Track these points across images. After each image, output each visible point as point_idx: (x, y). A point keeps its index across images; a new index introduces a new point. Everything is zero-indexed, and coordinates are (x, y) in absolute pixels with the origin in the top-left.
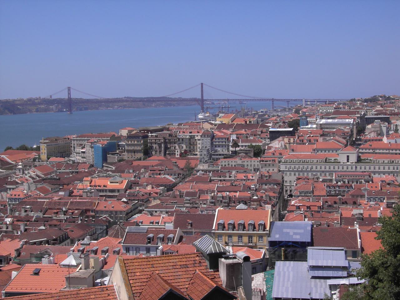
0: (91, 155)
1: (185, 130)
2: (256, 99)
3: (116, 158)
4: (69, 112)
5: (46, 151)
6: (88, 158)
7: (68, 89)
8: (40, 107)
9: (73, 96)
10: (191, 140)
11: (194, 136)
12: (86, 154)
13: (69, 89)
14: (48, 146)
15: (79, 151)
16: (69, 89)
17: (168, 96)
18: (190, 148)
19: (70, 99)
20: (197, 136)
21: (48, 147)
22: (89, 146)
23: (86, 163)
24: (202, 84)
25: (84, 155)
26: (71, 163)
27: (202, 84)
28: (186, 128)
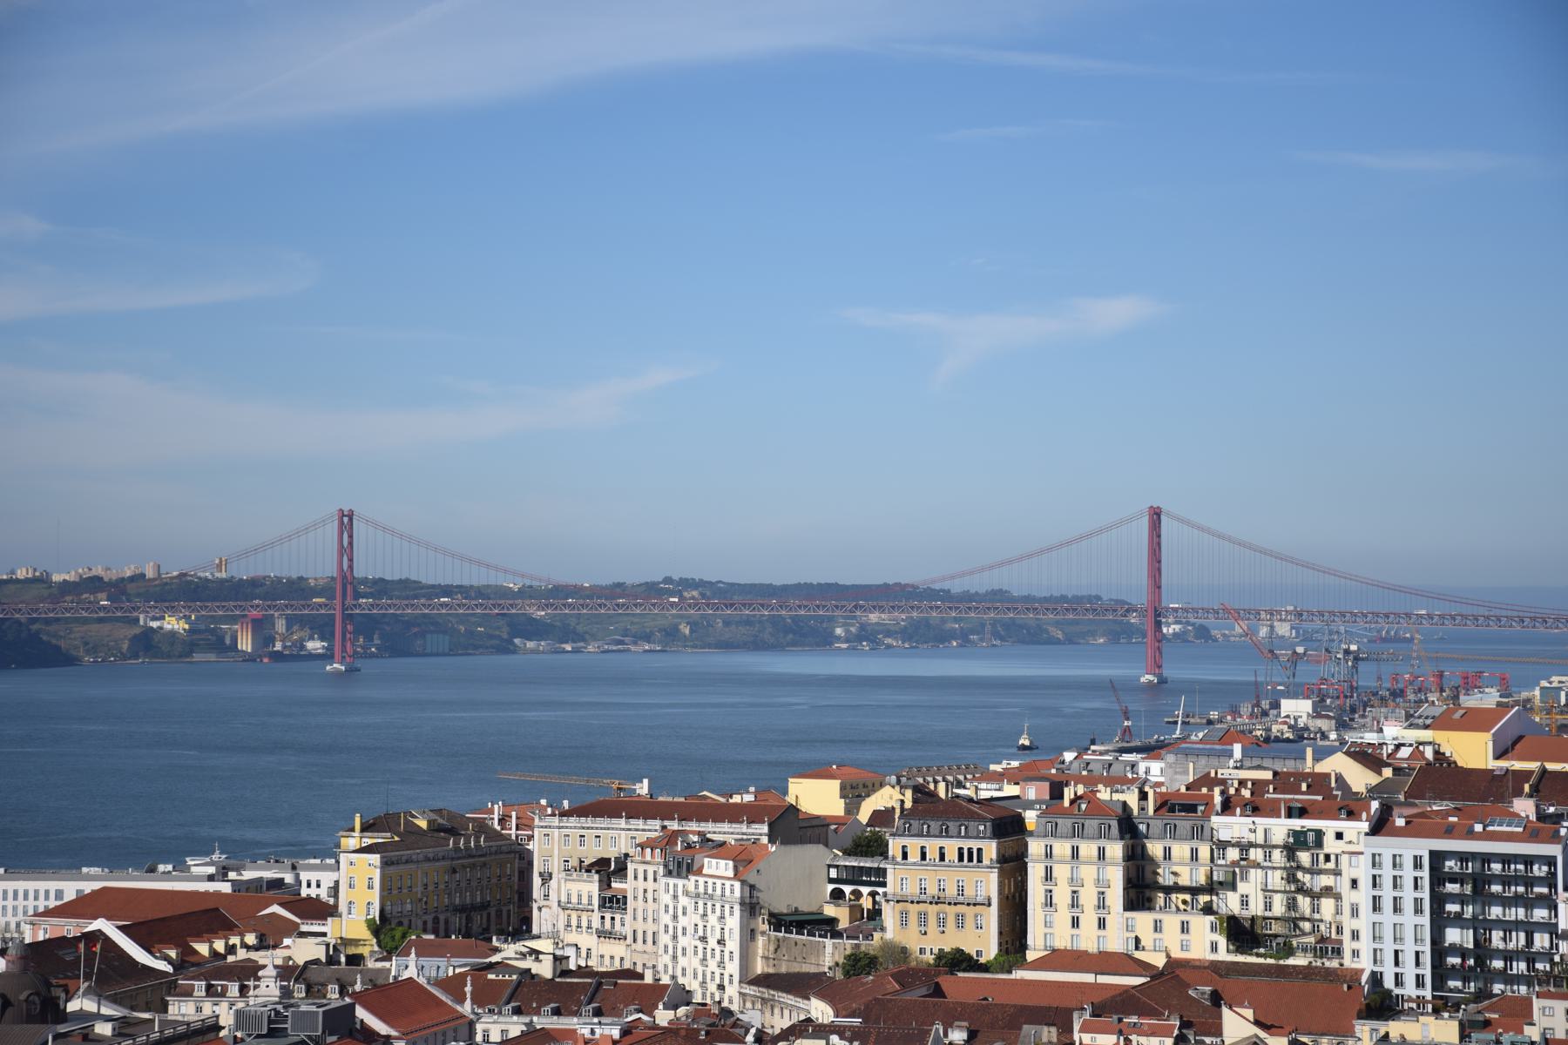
0: (662, 929)
1: (1246, 793)
2: (1498, 612)
3: (829, 949)
4: (341, 663)
5: (375, 897)
6: (639, 946)
7: (341, 523)
8: (161, 628)
9: (364, 568)
10: (1304, 857)
11: (1319, 834)
12: (628, 918)
13: (346, 521)
14: (393, 863)
15: (585, 901)
16: (346, 521)
17: (944, 579)
18: (1292, 905)
19: (347, 583)
20: (1339, 836)
21: (392, 870)
22: (651, 869)
23: (641, 976)
24: (1156, 515)
25: (618, 926)
26: (545, 969)
27: (1156, 515)
28: (1254, 782)
